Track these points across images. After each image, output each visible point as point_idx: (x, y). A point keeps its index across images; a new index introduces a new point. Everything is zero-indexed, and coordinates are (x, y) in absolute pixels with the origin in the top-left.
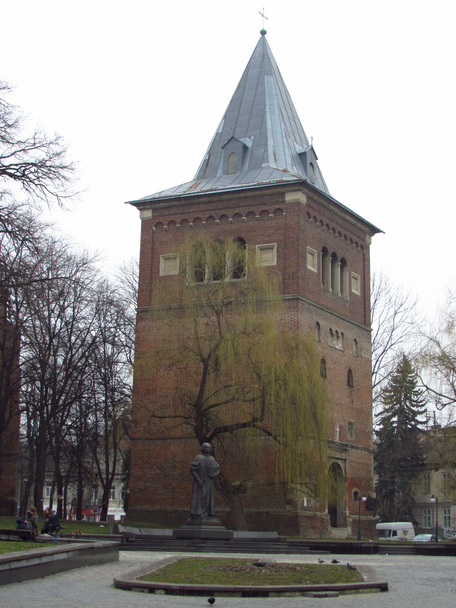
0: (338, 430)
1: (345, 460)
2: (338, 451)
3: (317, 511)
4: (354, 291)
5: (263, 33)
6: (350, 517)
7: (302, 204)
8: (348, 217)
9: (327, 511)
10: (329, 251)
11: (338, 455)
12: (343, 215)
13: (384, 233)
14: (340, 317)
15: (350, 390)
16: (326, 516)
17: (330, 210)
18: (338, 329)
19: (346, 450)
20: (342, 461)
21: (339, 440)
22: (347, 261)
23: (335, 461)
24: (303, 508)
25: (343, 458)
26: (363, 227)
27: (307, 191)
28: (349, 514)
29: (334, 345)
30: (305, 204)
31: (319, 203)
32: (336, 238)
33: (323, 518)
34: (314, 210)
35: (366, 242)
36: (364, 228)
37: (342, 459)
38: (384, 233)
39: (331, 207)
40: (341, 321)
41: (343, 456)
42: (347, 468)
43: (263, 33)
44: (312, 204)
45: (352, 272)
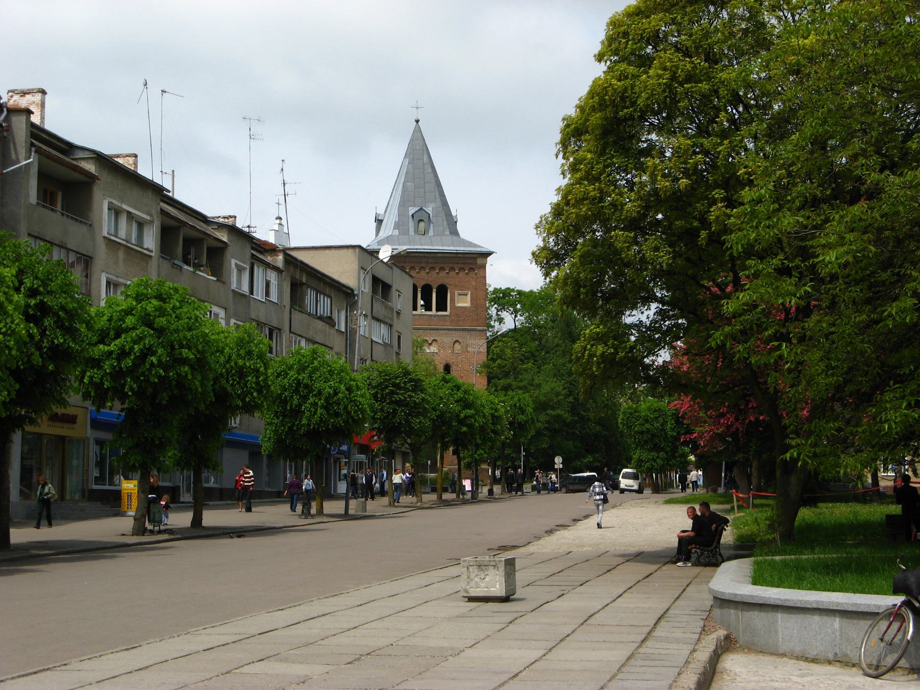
5: (417, 121)
12: (432, 255)
18: (428, 339)
40: (432, 331)
43: (417, 121)
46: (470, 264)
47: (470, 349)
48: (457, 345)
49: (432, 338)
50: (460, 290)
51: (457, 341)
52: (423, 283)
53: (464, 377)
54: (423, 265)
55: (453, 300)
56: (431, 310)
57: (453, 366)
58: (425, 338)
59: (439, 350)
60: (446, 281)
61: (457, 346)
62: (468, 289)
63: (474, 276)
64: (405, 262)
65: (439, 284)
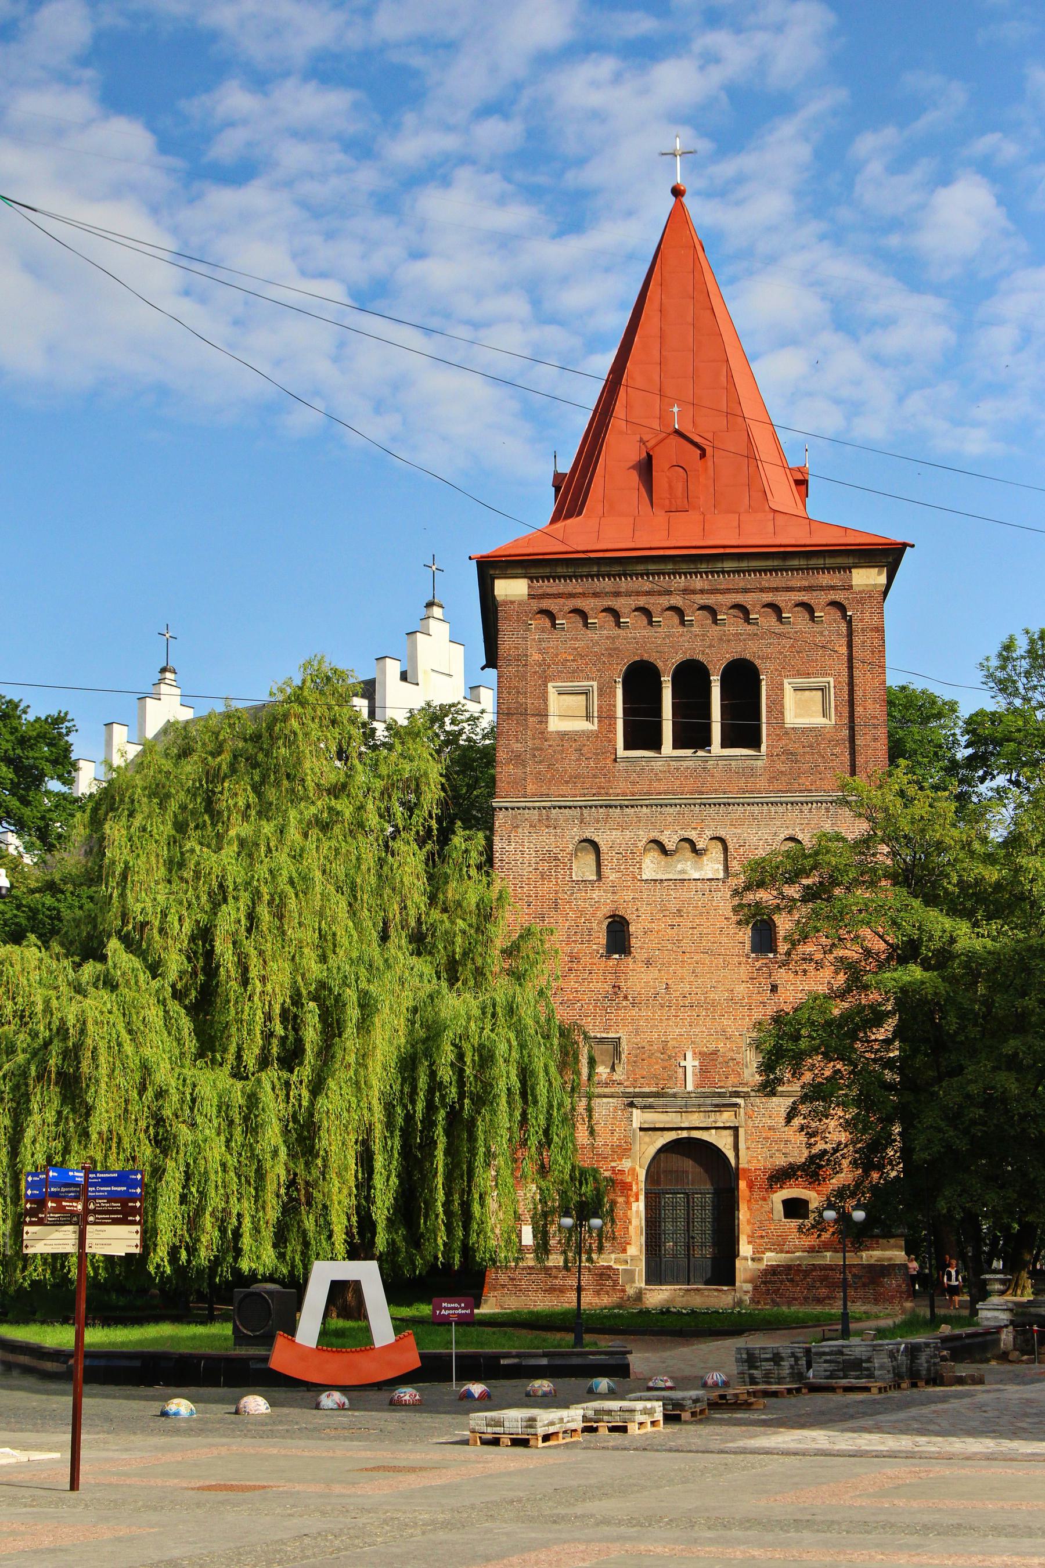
0: (691, 1063)
6: (760, 1260)
7: (512, 602)
10: (660, 664)
11: (695, 1119)
13: (913, 546)
15: (758, 964)
18: (693, 835)
22: (757, 662)
23: (684, 1134)
27: (520, 571)
29: (683, 872)
34: (571, 596)
35: (856, 589)
37: (717, 1128)
38: (913, 546)
41: (726, 1117)
42: (742, 1145)
45: (786, 681)
46: (833, 588)
49: (709, 833)
50: (799, 674)
52: (679, 658)
54: (677, 601)
56: (703, 741)
58: (687, 834)
60: (750, 651)
62: (830, 675)
64: (617, 594)
65: (729, 657)
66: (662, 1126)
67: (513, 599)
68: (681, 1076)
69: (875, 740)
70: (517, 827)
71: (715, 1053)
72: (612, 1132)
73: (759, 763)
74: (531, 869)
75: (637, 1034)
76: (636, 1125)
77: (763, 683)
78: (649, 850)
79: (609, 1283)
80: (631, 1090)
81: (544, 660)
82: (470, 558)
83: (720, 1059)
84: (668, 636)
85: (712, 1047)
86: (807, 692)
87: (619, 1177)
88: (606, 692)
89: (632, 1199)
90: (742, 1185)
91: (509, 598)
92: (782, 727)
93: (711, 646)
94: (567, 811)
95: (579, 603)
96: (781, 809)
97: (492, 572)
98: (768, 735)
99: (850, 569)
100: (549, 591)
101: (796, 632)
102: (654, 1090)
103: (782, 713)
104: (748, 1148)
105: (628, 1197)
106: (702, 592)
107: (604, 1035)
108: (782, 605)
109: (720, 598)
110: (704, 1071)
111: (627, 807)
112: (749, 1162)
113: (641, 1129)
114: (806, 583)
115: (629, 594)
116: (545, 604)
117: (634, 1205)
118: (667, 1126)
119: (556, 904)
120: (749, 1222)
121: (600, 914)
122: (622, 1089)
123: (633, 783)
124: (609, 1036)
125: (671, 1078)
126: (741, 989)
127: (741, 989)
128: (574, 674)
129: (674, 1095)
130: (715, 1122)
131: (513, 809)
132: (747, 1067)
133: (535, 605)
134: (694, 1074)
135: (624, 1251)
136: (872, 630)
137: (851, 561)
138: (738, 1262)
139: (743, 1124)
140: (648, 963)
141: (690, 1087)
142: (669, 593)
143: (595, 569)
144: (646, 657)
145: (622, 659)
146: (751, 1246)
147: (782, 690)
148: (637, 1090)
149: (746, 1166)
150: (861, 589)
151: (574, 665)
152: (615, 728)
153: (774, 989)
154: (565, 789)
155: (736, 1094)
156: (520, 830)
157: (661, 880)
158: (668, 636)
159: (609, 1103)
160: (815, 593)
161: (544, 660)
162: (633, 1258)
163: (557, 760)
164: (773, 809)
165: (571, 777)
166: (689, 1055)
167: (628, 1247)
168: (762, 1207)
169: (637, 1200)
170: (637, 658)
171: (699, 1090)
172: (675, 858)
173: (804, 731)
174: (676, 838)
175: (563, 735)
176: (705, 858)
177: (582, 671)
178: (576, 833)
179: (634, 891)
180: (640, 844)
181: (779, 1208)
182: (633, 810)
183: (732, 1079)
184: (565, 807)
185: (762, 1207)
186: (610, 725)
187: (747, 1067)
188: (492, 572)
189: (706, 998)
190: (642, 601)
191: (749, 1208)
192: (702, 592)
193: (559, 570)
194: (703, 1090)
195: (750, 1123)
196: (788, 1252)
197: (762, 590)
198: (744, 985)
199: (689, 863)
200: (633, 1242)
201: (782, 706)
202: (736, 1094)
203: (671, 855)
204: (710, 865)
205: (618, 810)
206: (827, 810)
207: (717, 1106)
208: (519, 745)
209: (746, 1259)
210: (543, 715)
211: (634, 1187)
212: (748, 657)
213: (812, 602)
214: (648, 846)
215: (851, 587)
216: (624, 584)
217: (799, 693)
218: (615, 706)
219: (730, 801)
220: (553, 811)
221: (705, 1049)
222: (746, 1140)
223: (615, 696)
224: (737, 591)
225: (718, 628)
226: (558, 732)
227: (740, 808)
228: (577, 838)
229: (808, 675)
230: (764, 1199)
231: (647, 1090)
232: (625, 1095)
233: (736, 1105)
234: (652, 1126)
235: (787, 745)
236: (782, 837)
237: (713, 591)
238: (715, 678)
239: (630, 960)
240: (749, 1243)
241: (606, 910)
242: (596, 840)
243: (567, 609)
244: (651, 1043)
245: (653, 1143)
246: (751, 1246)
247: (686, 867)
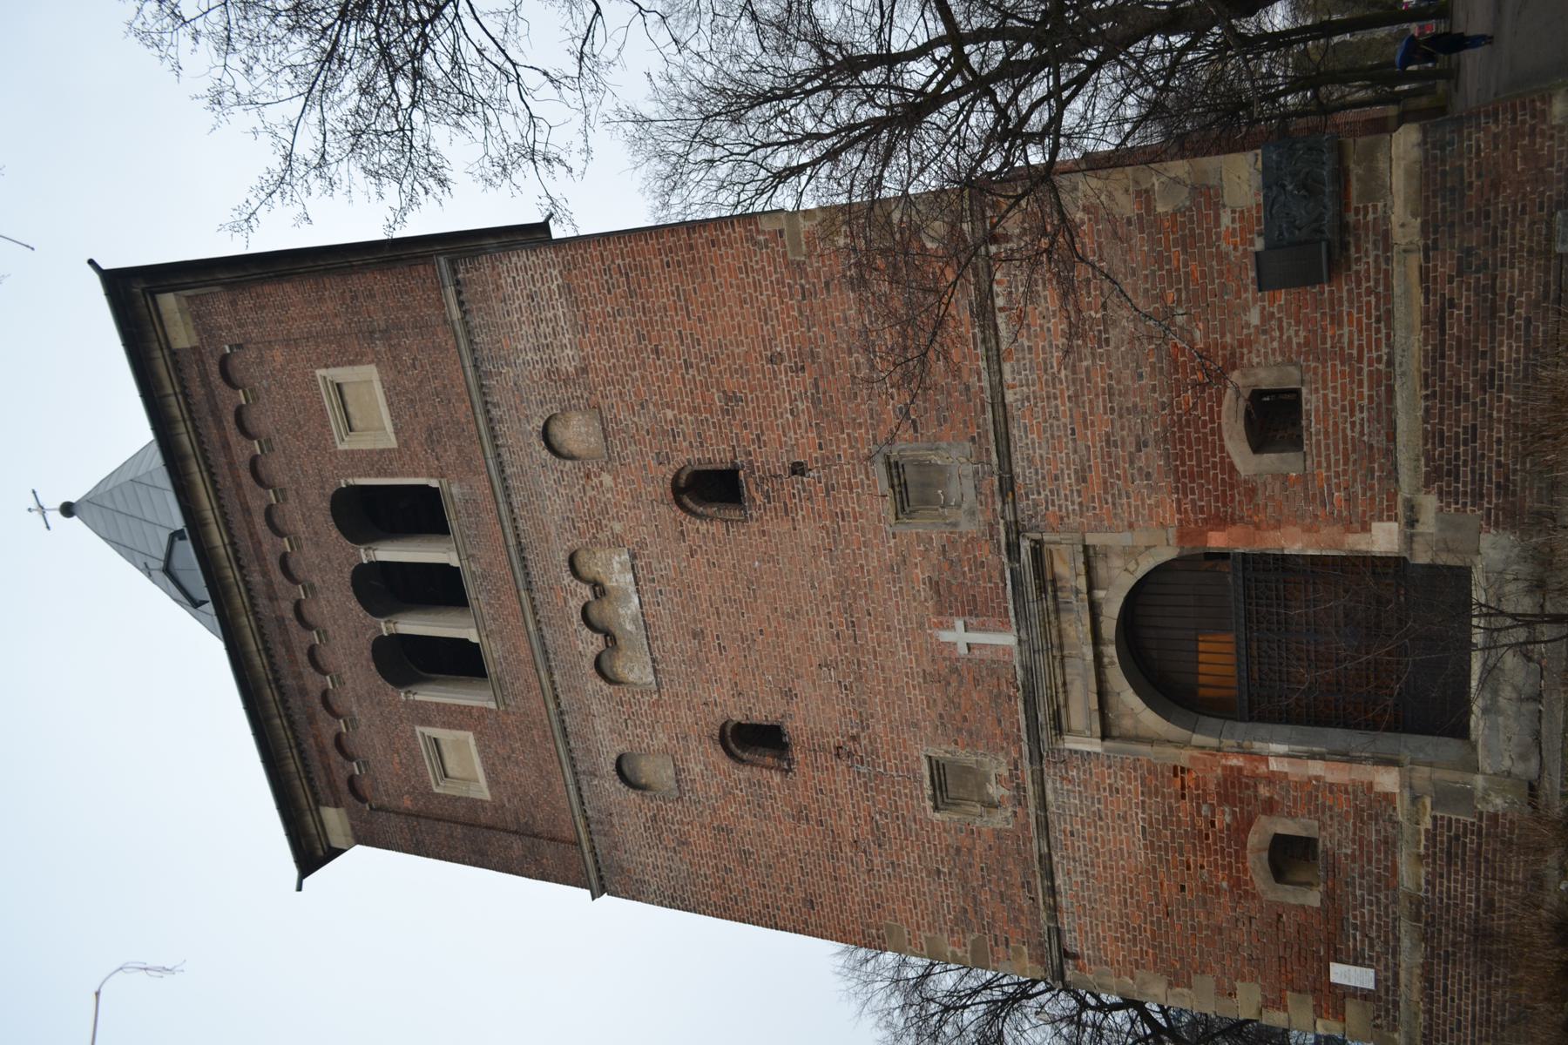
0: (958, 636)
1: (1086, 548)
2: (1060, 636)
3: (1394, 870)
4: (392, 443)
5: (68, 510)
6: (1411, 507)
7: (353, 827)
8: (217, 538)
9: (1387, 780)
10: (370, 635)
11: (1077, 629)
12: (231, 574)
13: (91, 262)
14: (529, 590)
16: (1415, 799)
17: (267, 650)
18: (575, 605)
19: (1038, 551)
20: (1101, 570)
21: (1003, 627)
22: (330, 491)
23: (1111, 651)
24: (1381, 1001)
25: (1082, 583)
26: (175, 408)
27: (309, 818)
28: (1393, 518)
29: (634, 620)
30: (342, 810)
31: (294, 732)
32: (312, 586)
33: (1432, 837)
34: (322, 751)
35: (195, 341)
36: (170, 391)
37: (1091, 587)
39: (257, 661)
41: (1067, 569)
42: (1125, 539)
43: (68, 510)
44: (321, 783)
47: (568, 360)
48: (560, 433)
49: (567, 578)
50: (325, 424)
51: (546, 435)
52: (354, 604)
53: (731, 383)
55: (377, 460)
57: (680, 459)
59: (617, 542)
61: (577, 433)
62: (314, 380)
63: (251, 354)
65: (335, 533)
66: (1094, 698)
67: (348, 827)
68: (987, 654)
69: (372, 296)
70: (622, 869)
71: (934, 585)
72: (1115, 790)
73: (455, 490)
74: (677, 859)
75: (916, 725)
76: (1095, 746)
77: (351, 482)
78: (615, 674)
79: (1471, 841)
80: (1025, 749)
81: (408, 792)
82: (299, 888)
83: (947, 575)
84: (335, 621)
85: (924, 591)
86: (351, 409)
87: (1212, 787)
88: (426, 715)
89: (1262, 769)
90: (1217, 540)
91: (349, 832)
92: (399, 451)
93: (330, 561)
94: (585, 795)
95: (329, 743)
96: (506, 456)
97: (321, 853)
98: (416, 475)
99: (174, 353)
100: (324, 779)
101: (278, 430)
102: (1021, 706)
103: (383, 451)
104: (1131, 526)
105: (1255, 777)
106: (265, 574)
107: (927, 782)
108: (247, 454)
109: (266, 547)
110: (975, 610)
111: (558, 705)
112: (1163, 526)
113: (1105, 736)
114: (210, 418)
115: (300, 676)
116: (344, 787)
117: (1274, 765)
118: (1093, 687)
119: (720, 829)
120: (1308, 530)
121: (726, 764)
122: (1026, 763)
123: (529, 688)
124: (927, 774)
125: (992, 672)
126: (808, 532)
127: (808, 532)
128: (415, 755)
129: (1028, 670)
130: (1077, 592)
131: (599, 870)
132: (955, 525)
133: (349, 798)
134: (982, 628)
135: (1388, 798)
136: (236, 311)
137: (158, 354)
138: (1422, 557)
139: (1077, 536)
140: (789, 694)
141: (1008, 639)
142: (280, 620)
143: (277, 721)
144: (368, 653)
145: (379, 686)
146: (1375, 526)
147: (352, 452)
148: (1025, 737)
149: (1172, 532)
150: (193, 333)
151: (404, 754)
152: (465, 707)
153: (798, 469)
154: (559, 788)
155: (1013, 550)
156: (625, 864)
157: (654, 660)
158: (335, 621)
159: (1055, 790)
160: (221, 405)
161: (408, 792)
162: (1408, 784)
163: (526, 794)
164: (508, 471)
165: (542, 777)
166: (946, 636)
167: (1378, 788)
168: (1272, 498)
169: (1264, 758)
170: (373, 667)
171: (1013, 620)
172: (618, 633)
173: (396, 416)
174: (586, 632)
175: (493, 781)
176: (608, 584)
177: (408, 744)
178: (611, 785)
179: (678, 705)
180: (608, 689)
181: (1269, 461)
182: (561, 696)
183: (985, 553)
184: (581, 796)
185: (1272, 498)
186: (462, 713)
187: (955, 525)
188: (321, 853)
189: (834, 598)
190: (303, 658)
191: (1278, 526)
192: (265, 574)
193: (292, 768)
194: (1012, 613)
195: (1074, 521)
196: (1392, 437)
197: (239, 486)
198: (800, 526)
199: (621, 611)
200: (1366, 778)
201: (371, 452)
202: (1013, 550)
203: (614, 640)
204: (615, 576)
205: (566, 718)
206: (489, 374)
207: (1041, 589)
208: (515, 845)
209: (1409, 539)
210: (474, 804)
211: (1235, 761)
212: (326, 505)
213: (232, 409)
214: (609, 674)
215: (194, 349)
216: (289, 682)
217: (356, 422)
218: (437, 704)
219: (512, 541)
220: (589, 813)
221: (930, 604)
222: (1110, 529)
223: (426, 702)
224: (250, 524)
225: (305, 549)
226: (490, 788)
227: (521, 524)
228: (618, 784)
229: (323, 410)
230: (1252, 492)
231: (1022, 717)
232: (1037, 756)
233: (1038, 551)
234: (1096, 717)
235: (421, 445)
236: (546, 454)
237: (261, 559)
238: (364, 556)
239: (788, 726)
240: (1365, 528)
241: (717, 756)
242: (614, 756)
243: (340, 758)
244: (931, 703)
245: (1133, 714)
246: (1375, 526)
247: (626, 613)
